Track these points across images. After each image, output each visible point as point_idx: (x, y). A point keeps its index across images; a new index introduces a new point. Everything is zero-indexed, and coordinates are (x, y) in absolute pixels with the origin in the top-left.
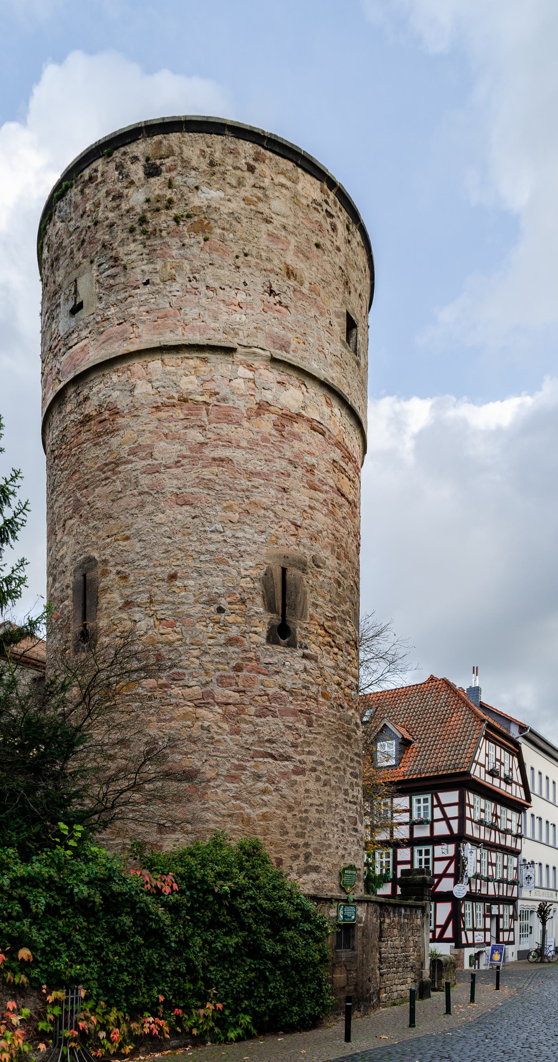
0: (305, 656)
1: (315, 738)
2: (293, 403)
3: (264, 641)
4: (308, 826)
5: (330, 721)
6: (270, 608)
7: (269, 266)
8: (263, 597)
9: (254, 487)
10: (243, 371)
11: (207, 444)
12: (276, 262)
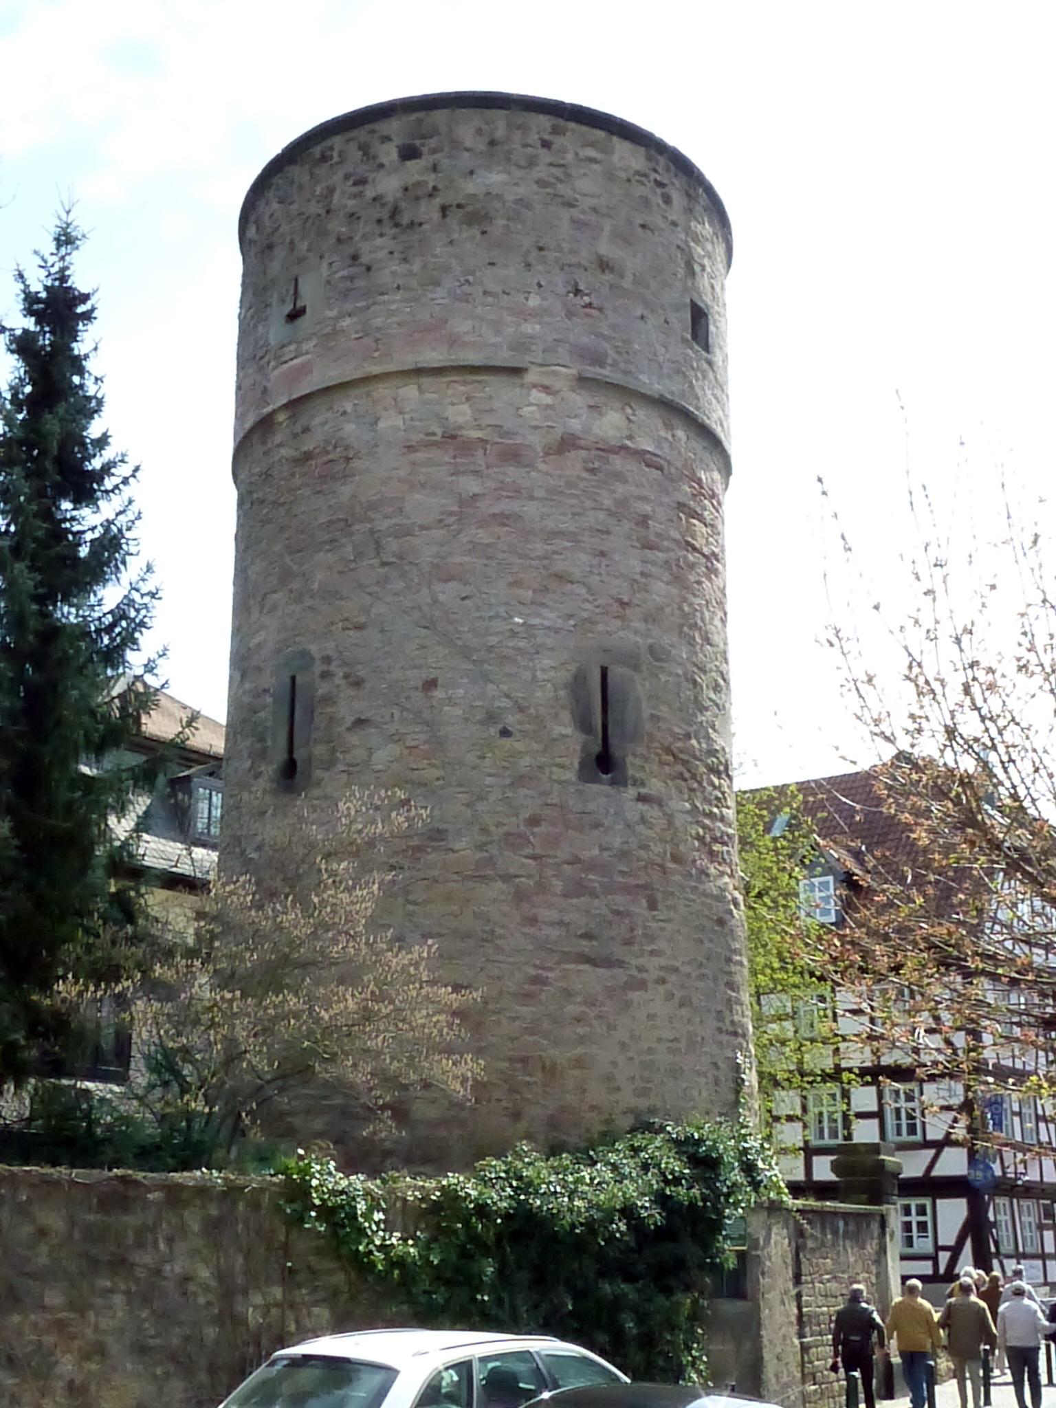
0: (641, 798)
1: (663, 929)
2: (611, 433)
3: (570, 775)
6: (584, 725)
7: (574, 260)
9: (555, 552)
10: (536, 395)
11: (484, 495)
12: (584, 253)
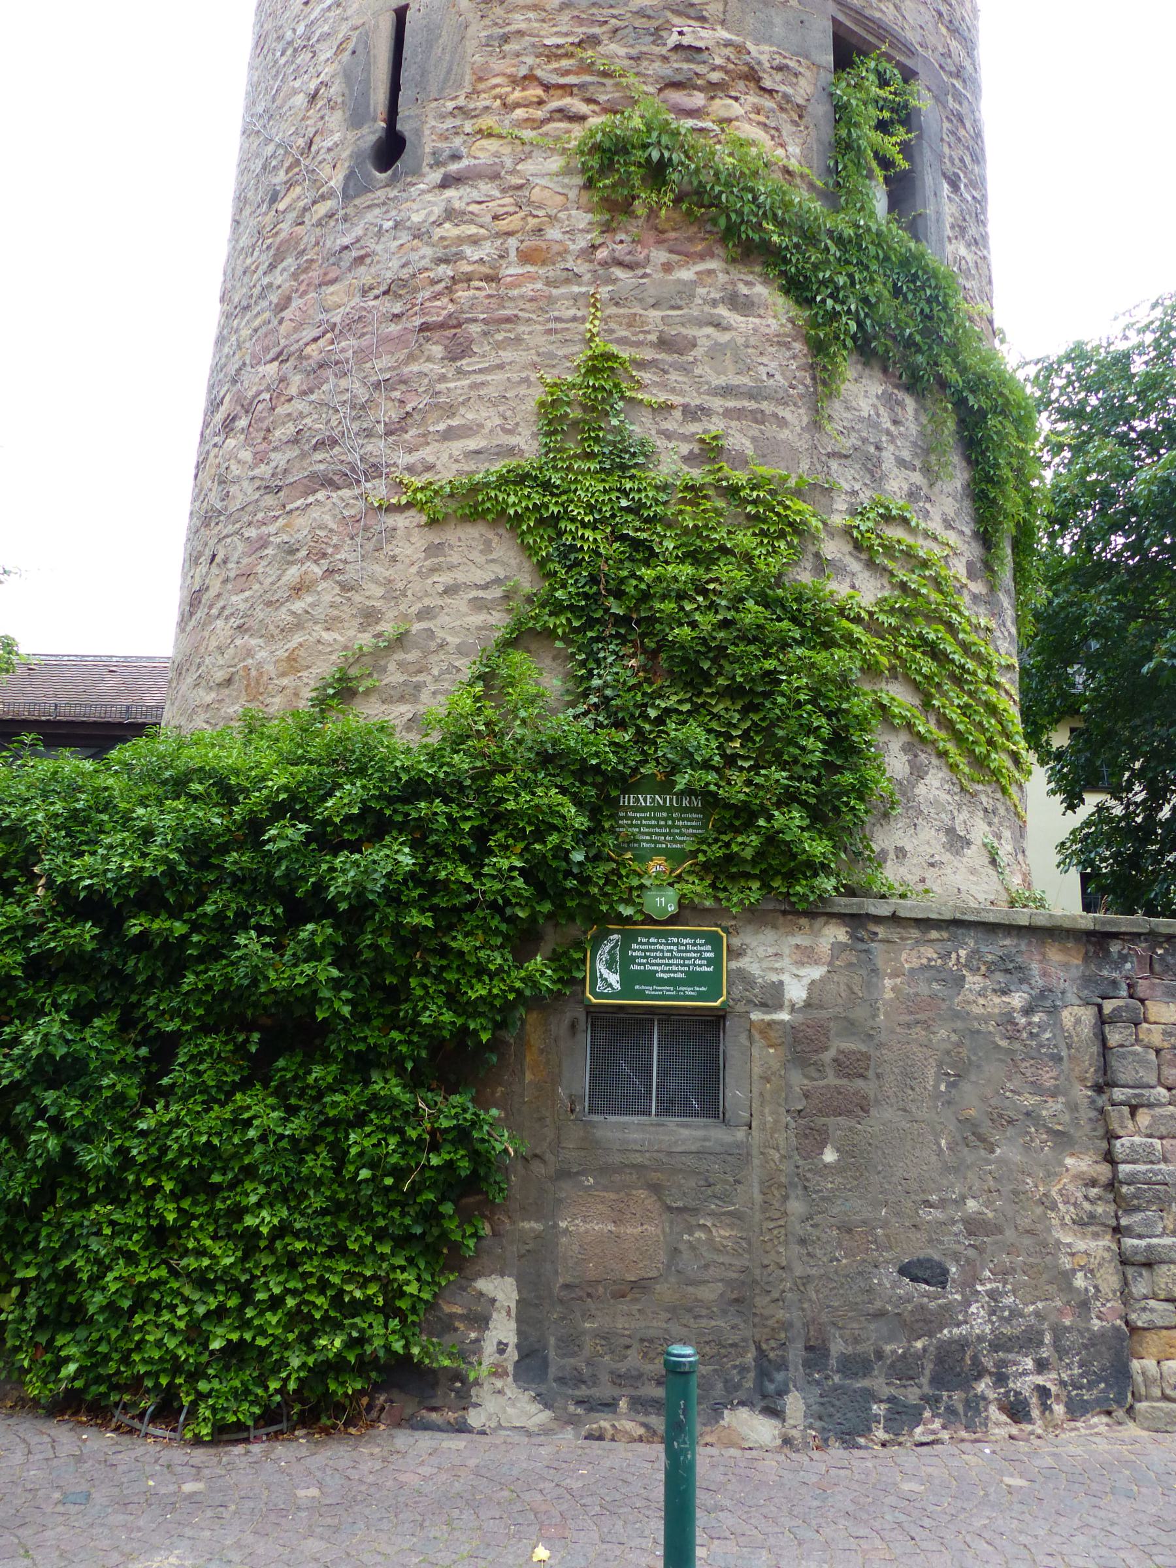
4: (433, 658)
5: (557, 319)
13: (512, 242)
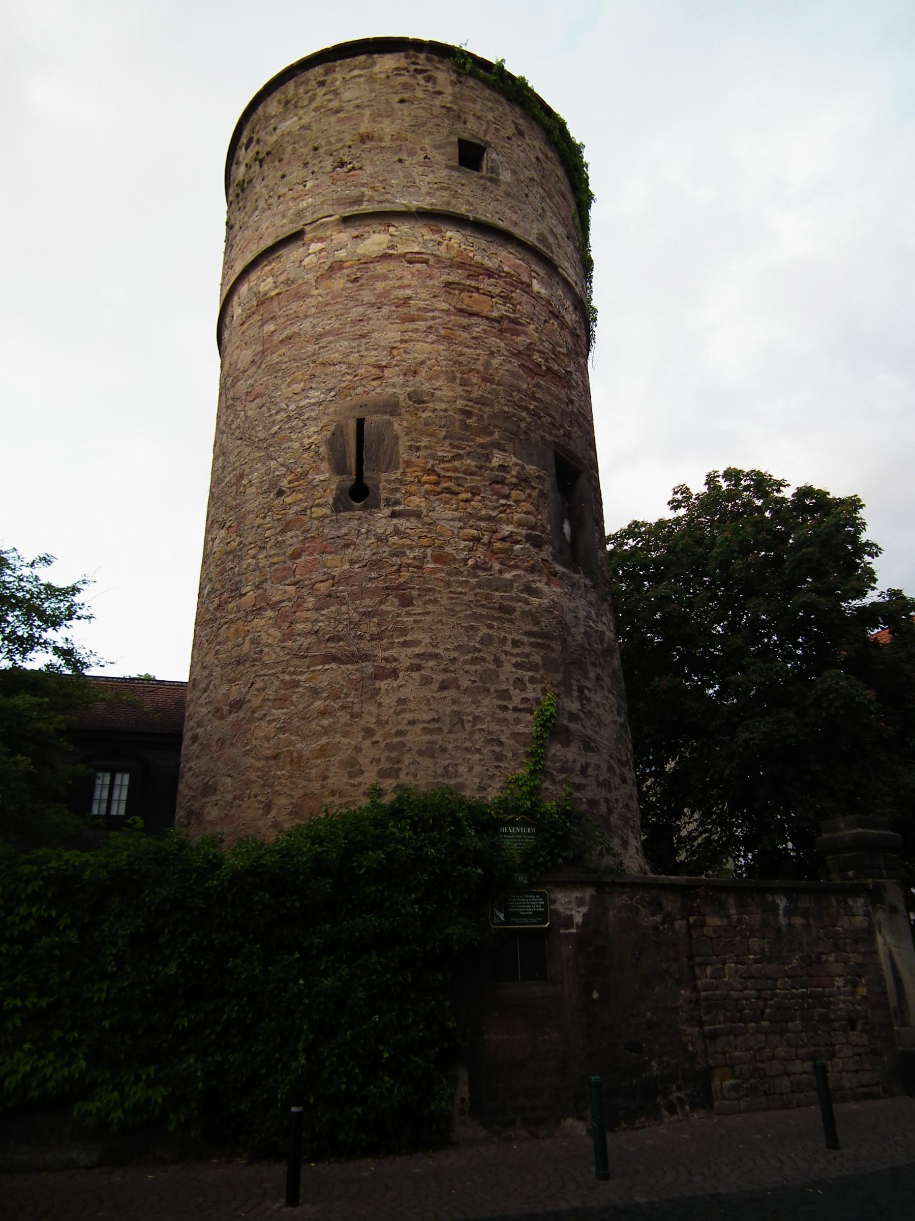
3: (329, 512)
6: (339, 468)
8: (329, 460)
13: (429, 551)
